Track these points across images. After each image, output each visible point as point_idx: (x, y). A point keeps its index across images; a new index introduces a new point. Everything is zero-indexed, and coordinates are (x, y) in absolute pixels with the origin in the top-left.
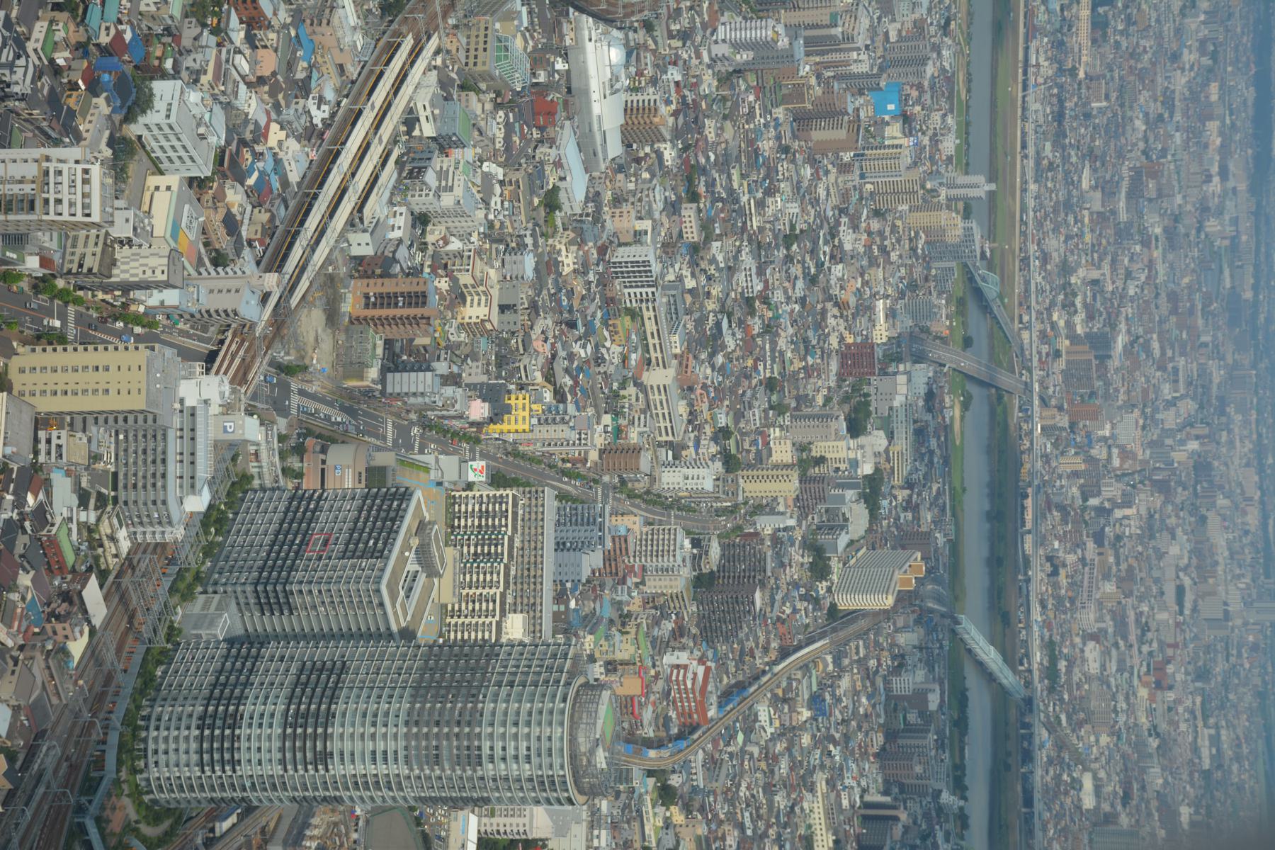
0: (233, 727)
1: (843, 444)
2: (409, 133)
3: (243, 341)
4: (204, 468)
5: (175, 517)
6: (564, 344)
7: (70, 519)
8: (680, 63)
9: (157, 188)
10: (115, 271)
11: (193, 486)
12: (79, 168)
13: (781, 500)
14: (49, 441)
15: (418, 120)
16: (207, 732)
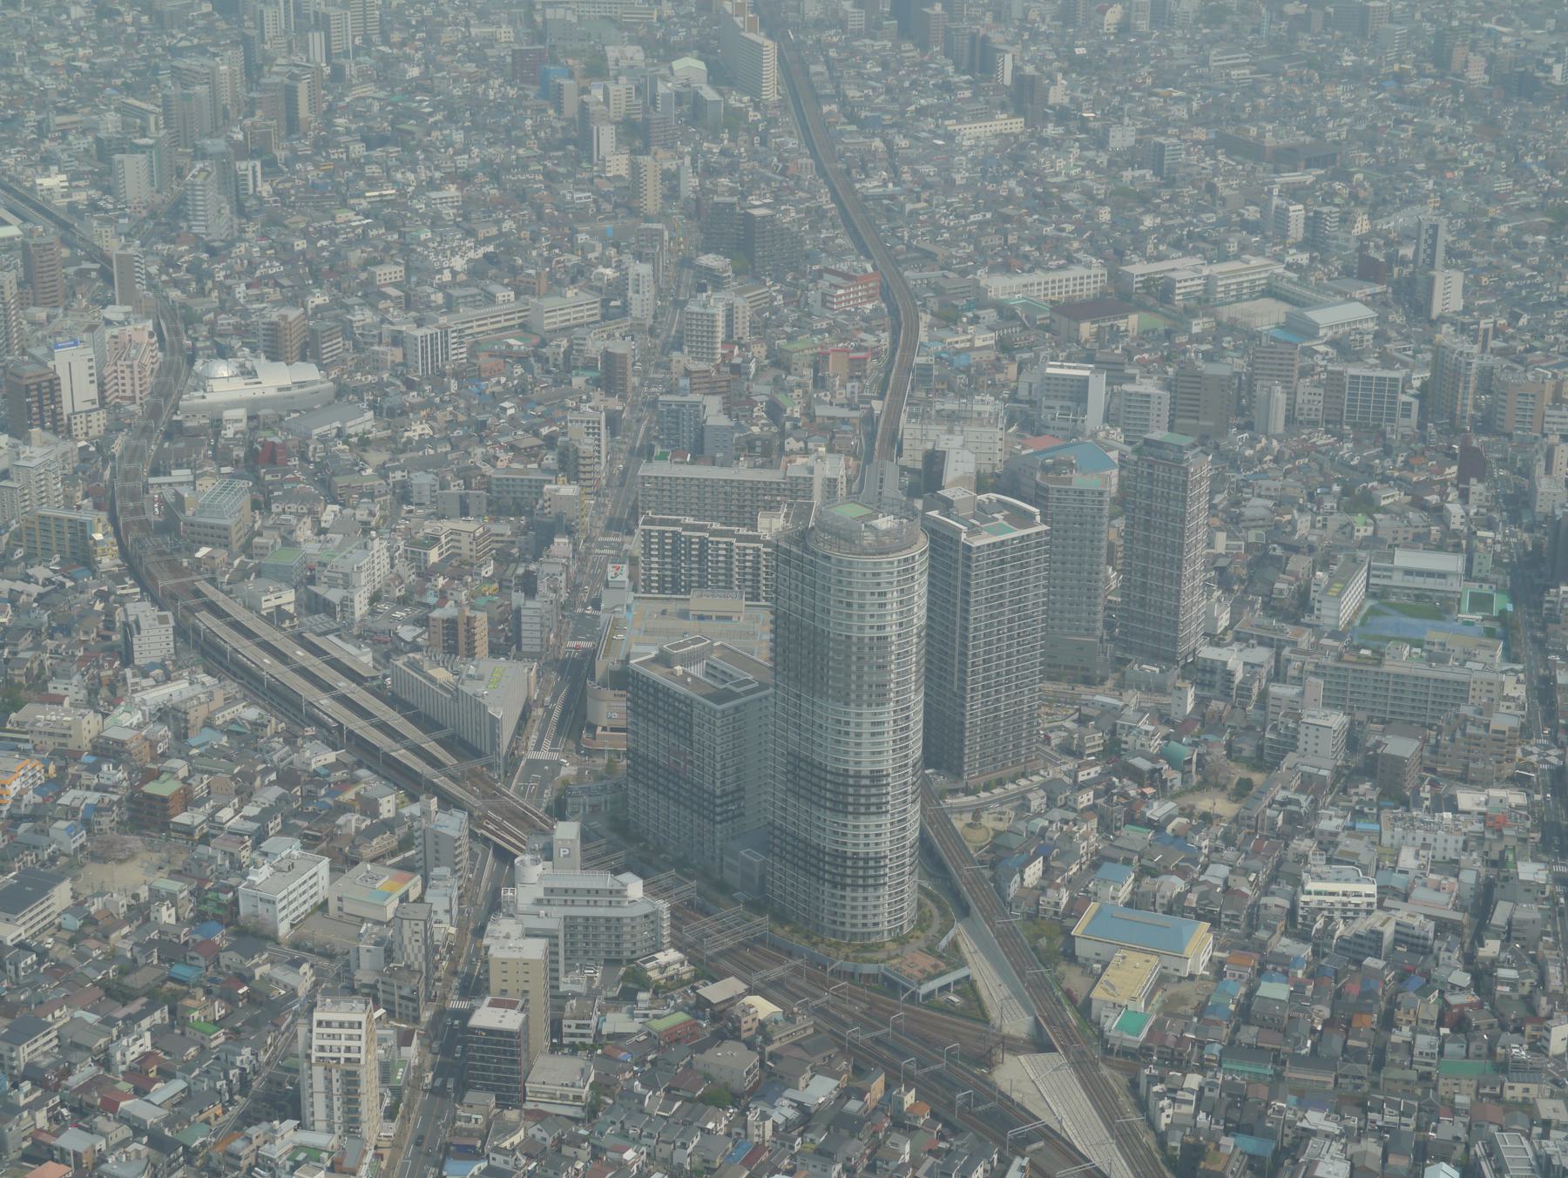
0: (845, 859)
1: (612, 88)
2: (291, 618)
3: (487, 817)
4: (601, 880)
5: (648, 909)
6: (502, 433)
7: (646, 1016)
8: (229, 282)
9: (340, 909)
10: (416, 966)
11: (618, 892)
12: (316, 1030)
13: (666, 165)
14: (572, 1035)
15: (278, 607)
16: (849, 881)
